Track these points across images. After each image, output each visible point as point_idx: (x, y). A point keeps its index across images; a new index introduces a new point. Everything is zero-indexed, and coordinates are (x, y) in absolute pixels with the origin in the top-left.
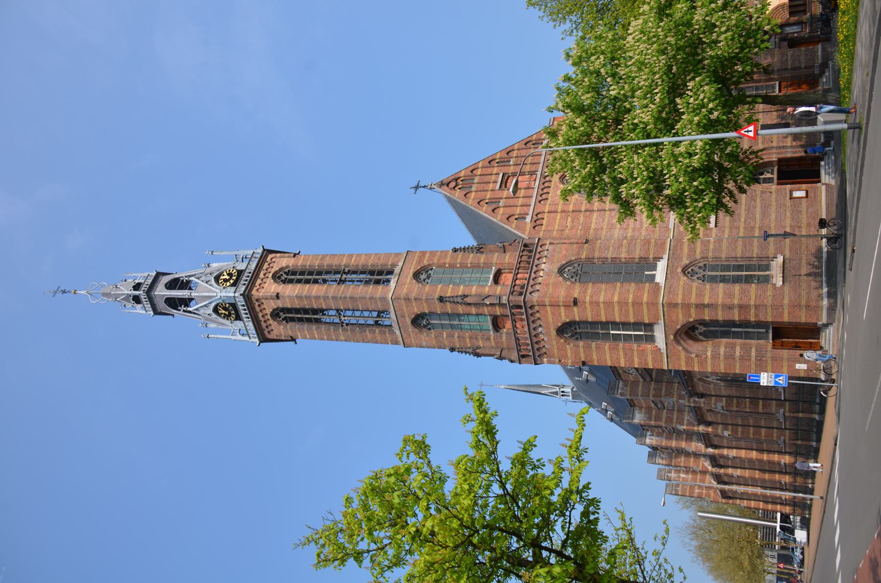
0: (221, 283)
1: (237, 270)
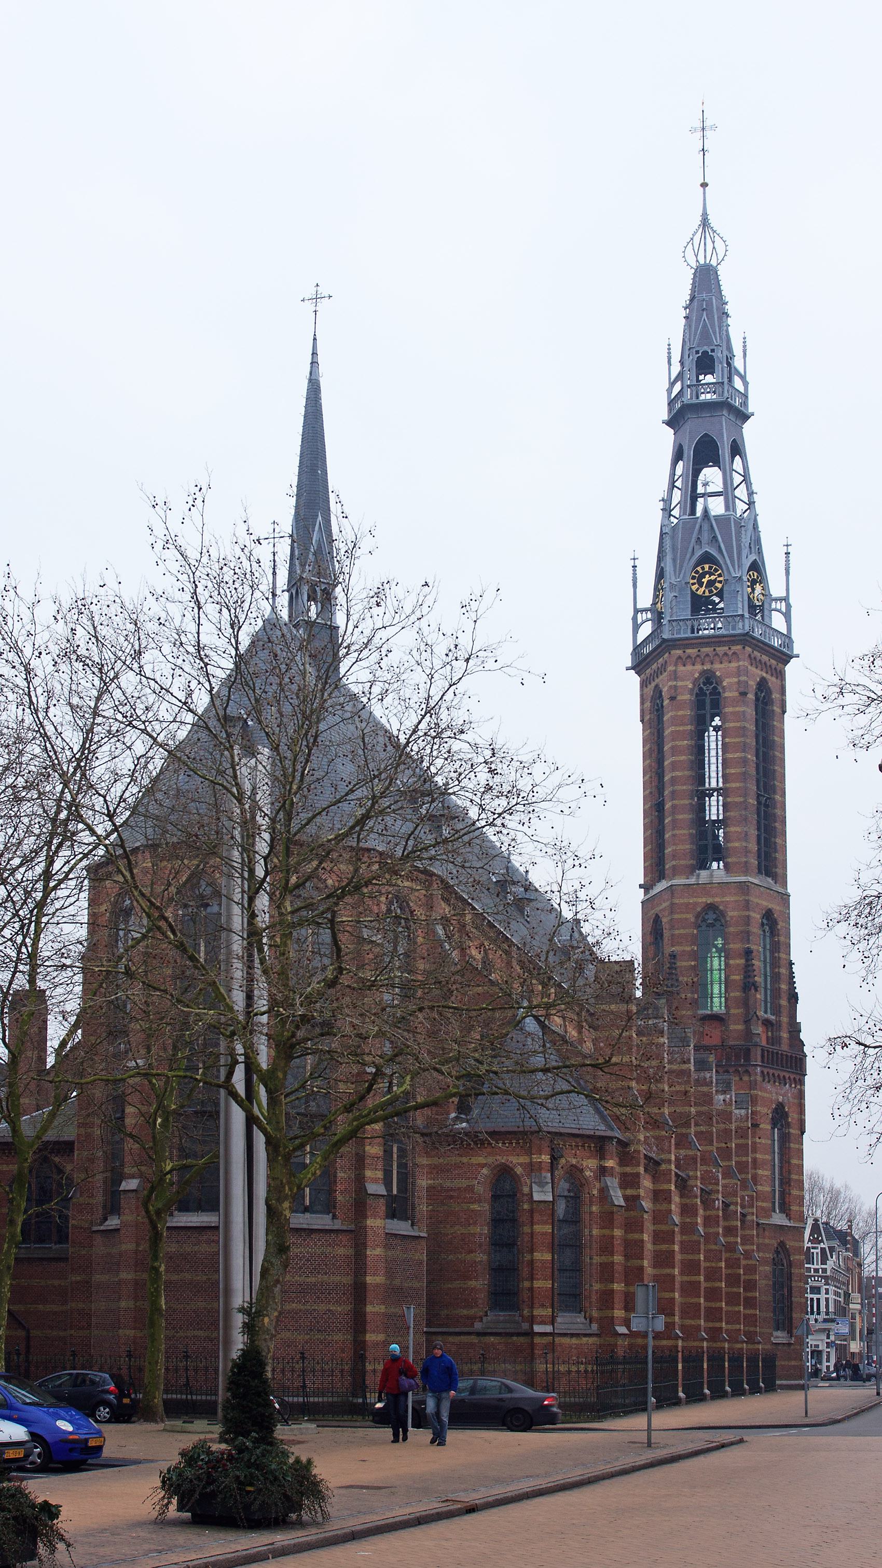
0: (697, 572)
1: (722, 589)
